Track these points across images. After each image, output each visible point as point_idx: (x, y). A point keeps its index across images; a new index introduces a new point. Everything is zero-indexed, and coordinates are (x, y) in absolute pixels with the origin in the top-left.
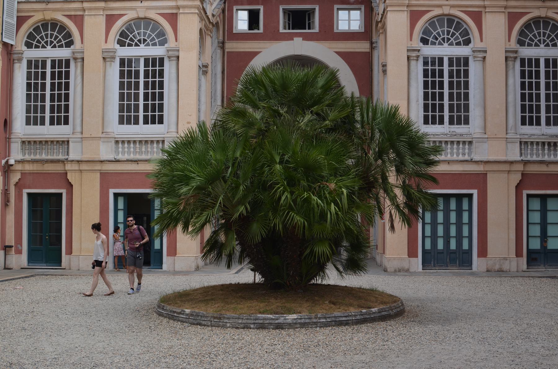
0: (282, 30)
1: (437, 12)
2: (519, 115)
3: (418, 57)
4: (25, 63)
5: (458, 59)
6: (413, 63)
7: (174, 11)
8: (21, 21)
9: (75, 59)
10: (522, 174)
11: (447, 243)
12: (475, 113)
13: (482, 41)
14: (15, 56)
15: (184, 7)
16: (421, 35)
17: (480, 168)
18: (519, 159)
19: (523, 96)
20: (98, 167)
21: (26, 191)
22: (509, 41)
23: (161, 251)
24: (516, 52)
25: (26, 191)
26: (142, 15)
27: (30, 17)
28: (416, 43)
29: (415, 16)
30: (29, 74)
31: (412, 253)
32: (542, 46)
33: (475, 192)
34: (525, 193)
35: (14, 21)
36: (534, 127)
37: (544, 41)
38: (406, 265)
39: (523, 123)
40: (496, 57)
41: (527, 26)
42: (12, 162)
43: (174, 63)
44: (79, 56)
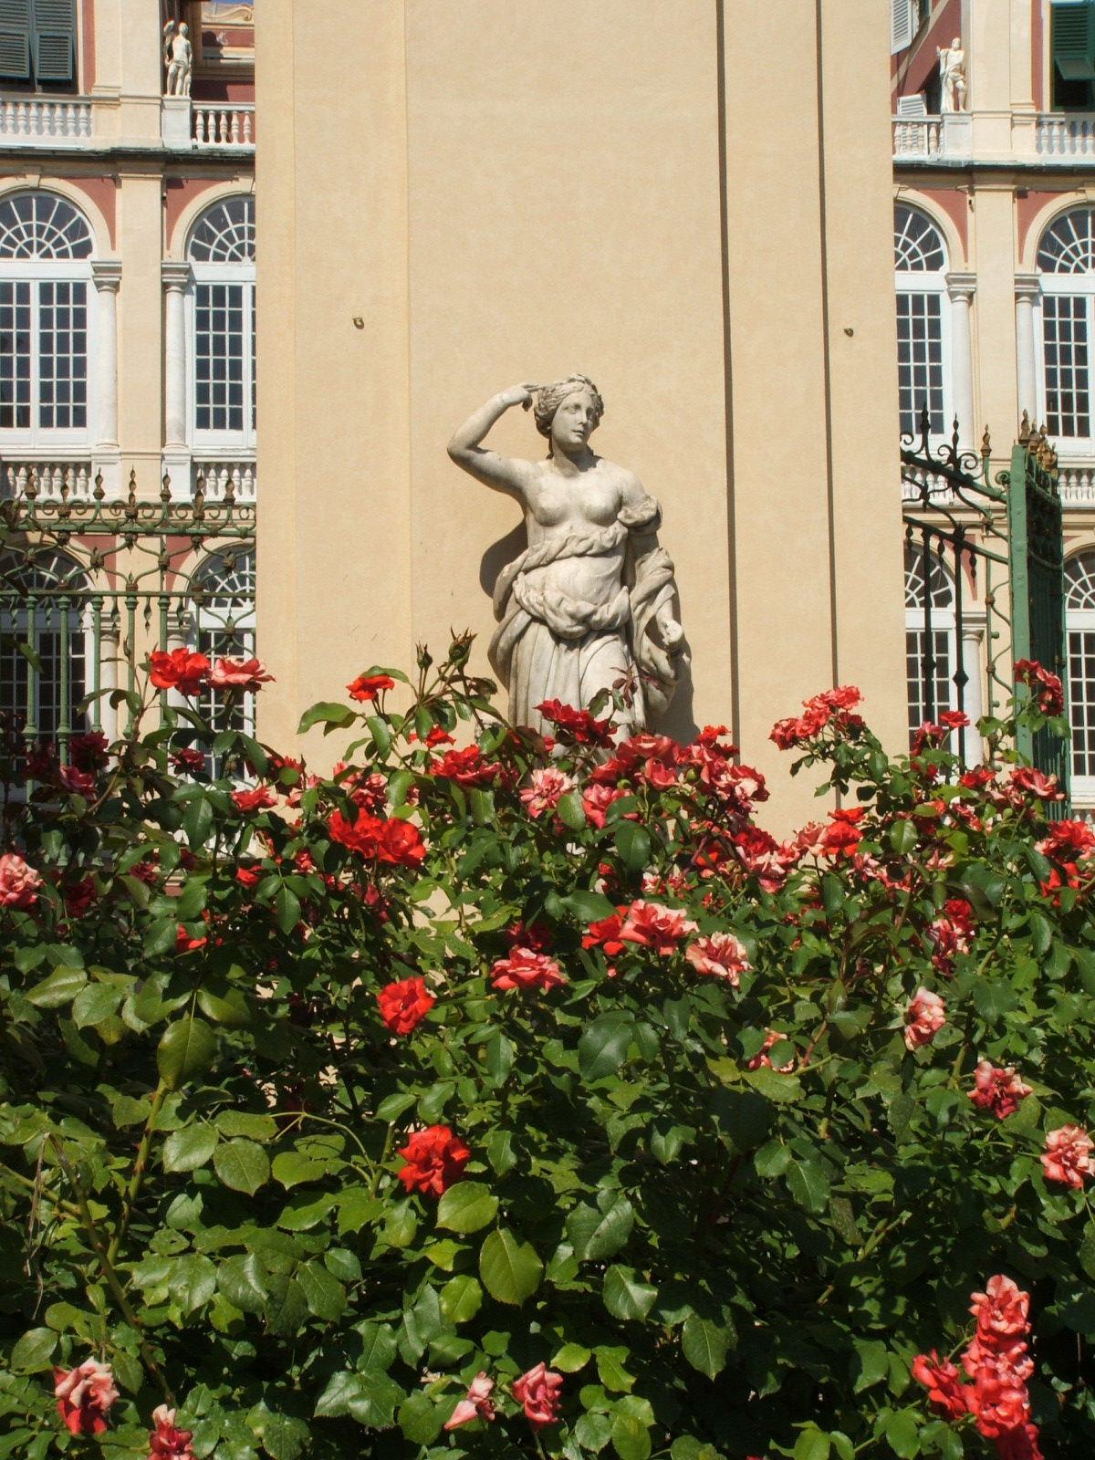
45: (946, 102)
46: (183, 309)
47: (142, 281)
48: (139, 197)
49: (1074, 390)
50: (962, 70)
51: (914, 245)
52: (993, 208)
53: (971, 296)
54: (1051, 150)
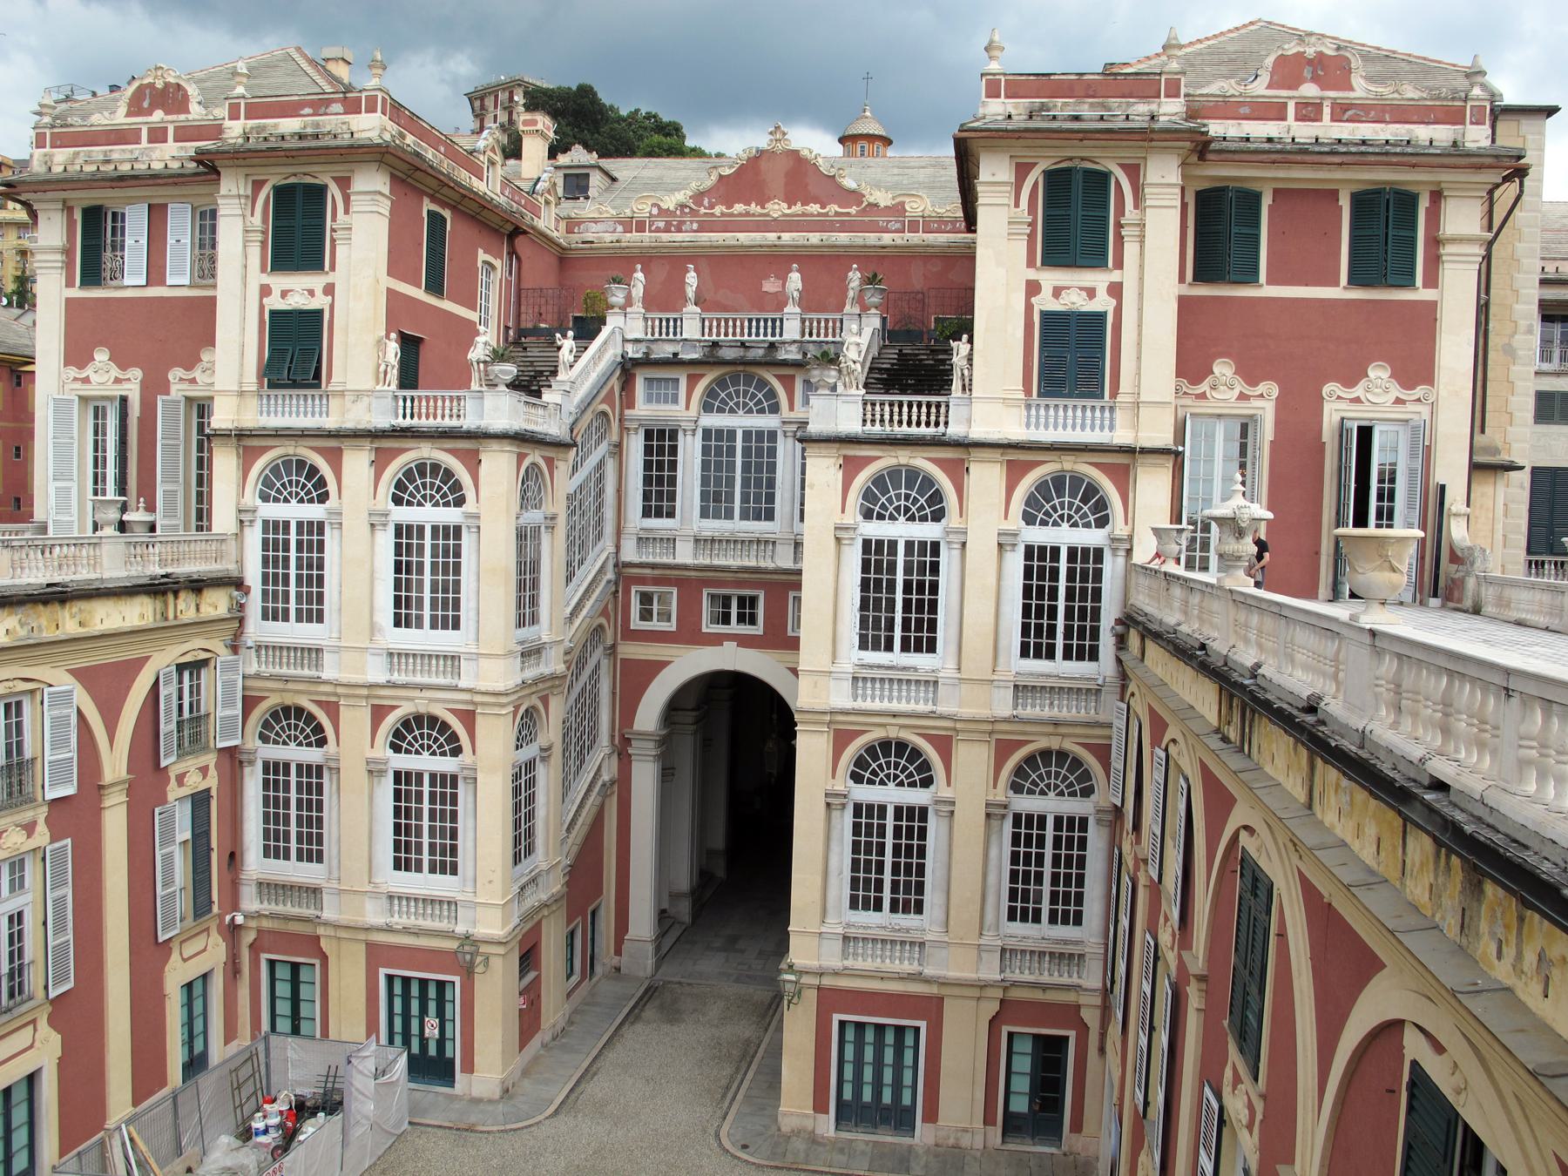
0: (708, 627)
1: (876, 734)
2: (1005, 904)
3: (844, 806)
4: (259, 766)
5: (911, 809)
6: (836, 814)
7: (471, 708)
8: (249, 703)
9: (330, 769)
10: (1002, 1001)
11: (878, 1093)
12: (931, 897)
13: (949, 784)
14: (244, 757)
15: (483, 704)
16: (852, 767)
17: (934, 990)
18: (998, 977)
19: (1014, 876)
20: (362, 936)
21: (264, 956)
22: (995, 787)
23: (452, 1061)
24: (1005, 807)
25: (264, 956)
26: (422, 710)
27: (264, 698)
28: (842, 783)
29: (841, 739)
30: (266, 783)
31: (820, 1106)
32: (1052, 794)
33: (923, 1025)
34: (1005, 1029)
35: (238, 711)
36: (1029, 925)
37: (1056, 786)
38: (809, 1124)
39: (1012, 917)
40: (970, 816)
41: (1030, 760)
42: (240, 919)
43: (471, 787)
44: (333, 765)
45: (956, 385)
46: (386, 540)
47: (355, 523)
48: (357, 462)
49: (1045, 622)
50: (970, 359)
51: (922, 501)
52: (986, 477)
53: (964, 544)
54: (1037, 426)
